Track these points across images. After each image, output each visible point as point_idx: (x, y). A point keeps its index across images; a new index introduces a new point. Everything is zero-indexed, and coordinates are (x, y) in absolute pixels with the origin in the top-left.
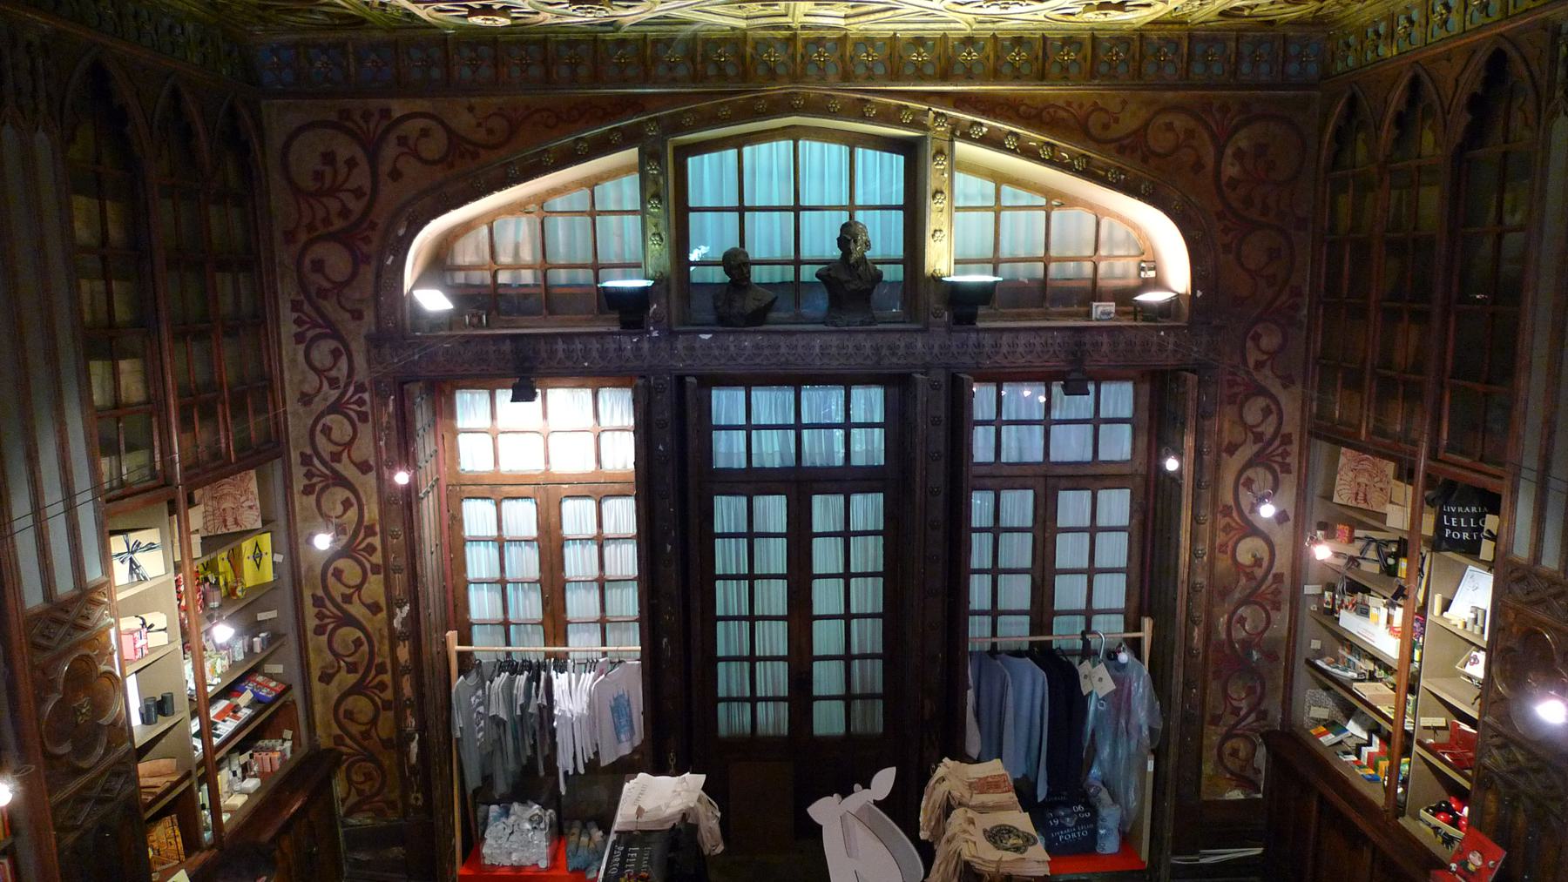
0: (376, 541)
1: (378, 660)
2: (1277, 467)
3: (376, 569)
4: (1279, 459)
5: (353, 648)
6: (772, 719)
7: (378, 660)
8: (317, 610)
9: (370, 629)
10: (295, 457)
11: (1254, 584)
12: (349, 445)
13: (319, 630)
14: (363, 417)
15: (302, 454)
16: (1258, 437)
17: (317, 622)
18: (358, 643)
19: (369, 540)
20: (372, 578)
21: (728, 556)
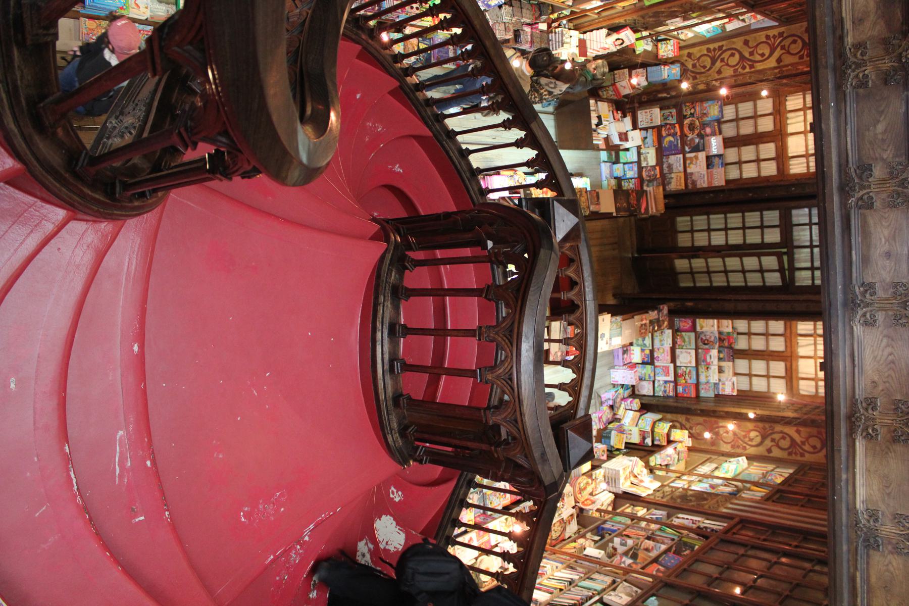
0: (747, 70)
1: (698, 76)
2: (790, 450)
3: (735, 71)
4: (794, 451)
5: (702, 65)
6: (684, 240)
7: (698, 76)
8: (717, 47)
9: (710, 72)
10: (782, 29)
11: (742, 438)
12: (789, 53)
13: (708, 50)
14: (801, 57)
15: (783, 32)
16: (803, 443)
17: (712, 48)
18: (704, 67)
19: (748, 67)
20: (732, 69)
21: (753, 218)
